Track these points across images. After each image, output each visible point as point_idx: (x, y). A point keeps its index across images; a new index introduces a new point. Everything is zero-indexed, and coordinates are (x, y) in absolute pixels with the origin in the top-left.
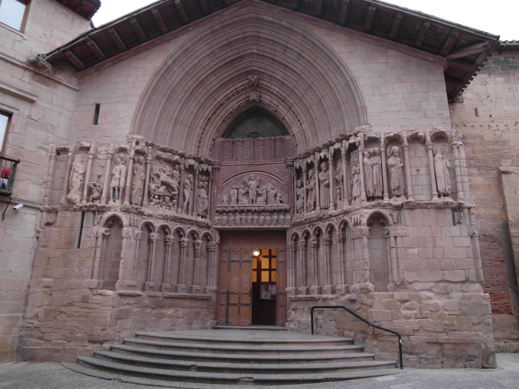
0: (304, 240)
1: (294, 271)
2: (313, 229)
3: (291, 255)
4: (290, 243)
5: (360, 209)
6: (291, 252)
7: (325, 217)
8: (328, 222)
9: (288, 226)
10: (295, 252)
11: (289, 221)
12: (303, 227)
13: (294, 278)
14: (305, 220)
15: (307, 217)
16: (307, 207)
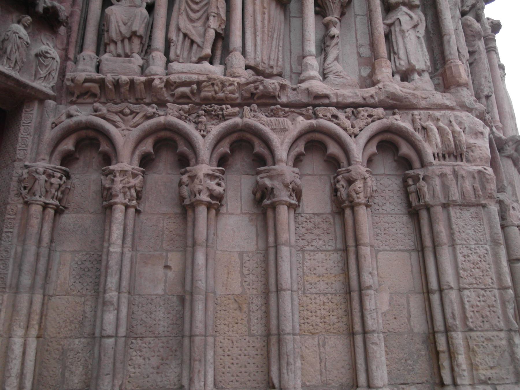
0: (135, 166)
1: (37, 307)
2: (216, 129)
3: (35, 222)
4: (41, 165)
5: (452, 109)
6: (36, 209)
7: (284, 99)
8: (303, 122)
9: (44, 86)
10: (59, 212)
11: (56, 65)
12: (150, 110)
13: (33, 344)
14: (168, 84)
15: (184, 77)
16: (168, 43)
